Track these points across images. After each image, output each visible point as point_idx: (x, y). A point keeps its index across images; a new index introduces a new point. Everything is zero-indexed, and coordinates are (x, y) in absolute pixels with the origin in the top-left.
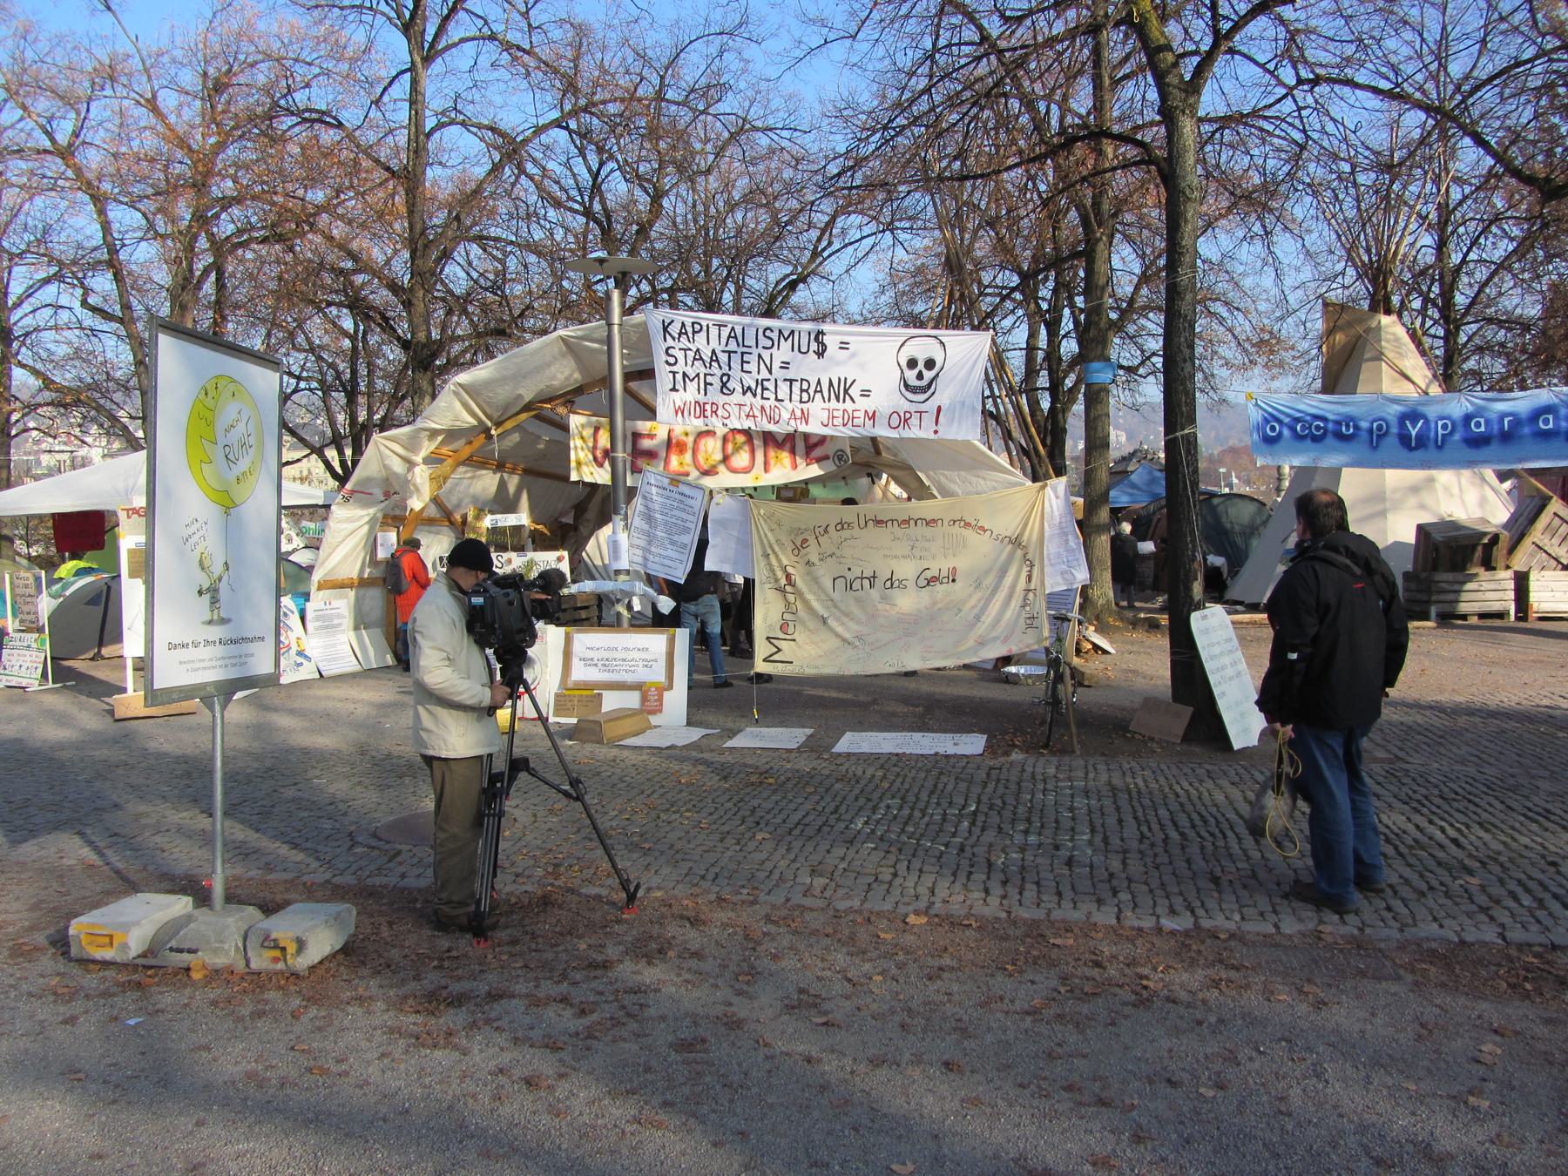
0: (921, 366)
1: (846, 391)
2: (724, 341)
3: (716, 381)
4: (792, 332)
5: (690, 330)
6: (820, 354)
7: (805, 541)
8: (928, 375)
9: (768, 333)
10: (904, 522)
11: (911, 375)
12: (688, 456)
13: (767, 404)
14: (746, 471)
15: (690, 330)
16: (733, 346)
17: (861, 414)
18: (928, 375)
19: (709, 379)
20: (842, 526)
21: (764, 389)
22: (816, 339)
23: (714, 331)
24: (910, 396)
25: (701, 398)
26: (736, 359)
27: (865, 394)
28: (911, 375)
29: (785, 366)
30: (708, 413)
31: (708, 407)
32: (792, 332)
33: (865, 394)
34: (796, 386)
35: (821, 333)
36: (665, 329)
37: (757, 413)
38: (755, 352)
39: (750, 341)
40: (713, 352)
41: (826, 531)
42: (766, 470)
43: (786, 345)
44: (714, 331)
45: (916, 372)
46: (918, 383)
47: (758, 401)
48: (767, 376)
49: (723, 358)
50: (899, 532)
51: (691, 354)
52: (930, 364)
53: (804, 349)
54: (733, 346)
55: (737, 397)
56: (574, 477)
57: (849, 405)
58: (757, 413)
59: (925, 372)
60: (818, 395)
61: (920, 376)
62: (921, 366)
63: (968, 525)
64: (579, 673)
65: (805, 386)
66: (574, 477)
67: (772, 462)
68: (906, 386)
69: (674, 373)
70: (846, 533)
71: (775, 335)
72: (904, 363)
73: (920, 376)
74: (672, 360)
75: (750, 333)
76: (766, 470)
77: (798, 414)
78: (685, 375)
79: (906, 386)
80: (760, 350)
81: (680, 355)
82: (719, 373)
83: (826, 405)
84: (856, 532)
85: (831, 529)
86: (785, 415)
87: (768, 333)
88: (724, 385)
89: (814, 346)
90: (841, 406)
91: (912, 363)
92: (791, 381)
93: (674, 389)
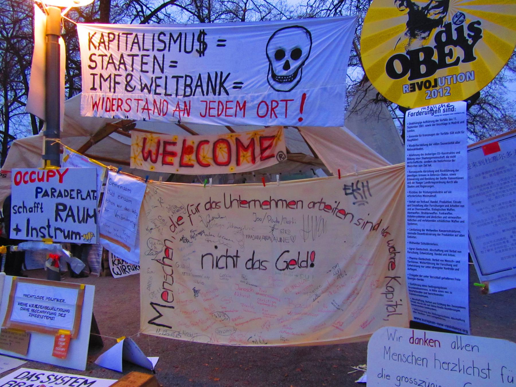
0: (288, 56)
1: (222, 84)
2: (129, 46)
3: (121, 80)
4: (180, 34)
5: (106, 39)
6: (201, 53)
7: (180, 218)
8: (294, 65)
9: (162, 37)
10: (266, 203)
11: (278, 66)
12: (193, 157)
13: (157, 98)
14: (227, 164)
15: (106, 39)
16: (135, 51)
17: (233, 105)
18: (294, 65)
19: (118, 79)
20: (211, 205)
21: (157, 86)
22: (199, 40)
23: (123, 38)
24: (278, 86)
25: (111, 95)
26: (138, 60)
27: (238, 86)
28: (278, 66)
29: (174, 64)
30: (115, 108)
31: (115, 102)
32: (180, 34)
33: (238, 86)
34: (182, 81)
35: (203, 33)
36: (90, 41)
37: (151, 107)
38: (151, 53)
39: (148, 45)
40: (122, 56)
41: (197, 210)
42: (238, 164)
43: (175, 47)
44: (123, 38)
45: (283, 62)
46: (285, 73)
47: (151, 97)
48: (160, 75)
49: (128, 60)
50: (261, 212)
51: (106, 59)
52: (296, 54)
53: (189, 49)
54: (135, 51)
55: (137, 94)
57: (223, 97)
58: (151, 107)
59: (291, 61)
60: (199, 90)
61: (287, 66)
62: (288, 56)
63: (328, 207)
64: (20, 316)
65: (188, 82)
67: (241, 159)
68: (274, 76)
69: (94, 75)
70: (214, 212)
71: (166, 39)
72: (272, 52)
73: (287, 66)
74: (93, 65)
75: (149, 37)
76: (238, 164)
77: (182, 106)
78: (101, 76)
79: (274, 76)
80: (156, 52)
81: (98, 59)
82: (124, 74)
83: (205, 98)
84: (222, 211)
85: (201, 208)
86: (172, 108)
87: (162, 37)
88: (128, 84)
89: (197, 46)
90: (216, 98)
91: (280, 54)
92: (177, 78)
93: (94, 89)
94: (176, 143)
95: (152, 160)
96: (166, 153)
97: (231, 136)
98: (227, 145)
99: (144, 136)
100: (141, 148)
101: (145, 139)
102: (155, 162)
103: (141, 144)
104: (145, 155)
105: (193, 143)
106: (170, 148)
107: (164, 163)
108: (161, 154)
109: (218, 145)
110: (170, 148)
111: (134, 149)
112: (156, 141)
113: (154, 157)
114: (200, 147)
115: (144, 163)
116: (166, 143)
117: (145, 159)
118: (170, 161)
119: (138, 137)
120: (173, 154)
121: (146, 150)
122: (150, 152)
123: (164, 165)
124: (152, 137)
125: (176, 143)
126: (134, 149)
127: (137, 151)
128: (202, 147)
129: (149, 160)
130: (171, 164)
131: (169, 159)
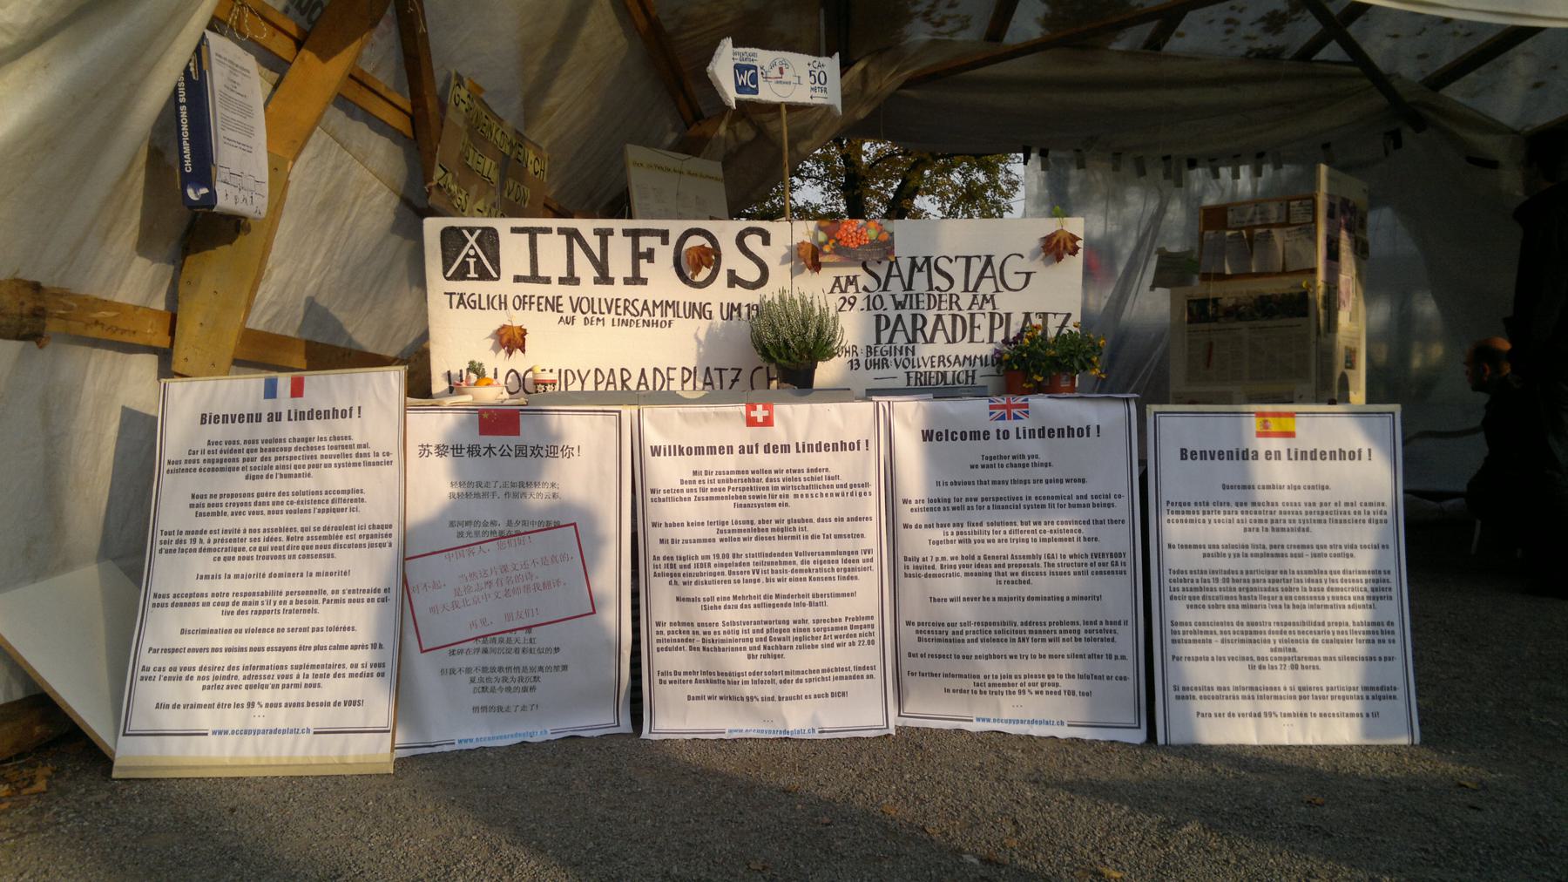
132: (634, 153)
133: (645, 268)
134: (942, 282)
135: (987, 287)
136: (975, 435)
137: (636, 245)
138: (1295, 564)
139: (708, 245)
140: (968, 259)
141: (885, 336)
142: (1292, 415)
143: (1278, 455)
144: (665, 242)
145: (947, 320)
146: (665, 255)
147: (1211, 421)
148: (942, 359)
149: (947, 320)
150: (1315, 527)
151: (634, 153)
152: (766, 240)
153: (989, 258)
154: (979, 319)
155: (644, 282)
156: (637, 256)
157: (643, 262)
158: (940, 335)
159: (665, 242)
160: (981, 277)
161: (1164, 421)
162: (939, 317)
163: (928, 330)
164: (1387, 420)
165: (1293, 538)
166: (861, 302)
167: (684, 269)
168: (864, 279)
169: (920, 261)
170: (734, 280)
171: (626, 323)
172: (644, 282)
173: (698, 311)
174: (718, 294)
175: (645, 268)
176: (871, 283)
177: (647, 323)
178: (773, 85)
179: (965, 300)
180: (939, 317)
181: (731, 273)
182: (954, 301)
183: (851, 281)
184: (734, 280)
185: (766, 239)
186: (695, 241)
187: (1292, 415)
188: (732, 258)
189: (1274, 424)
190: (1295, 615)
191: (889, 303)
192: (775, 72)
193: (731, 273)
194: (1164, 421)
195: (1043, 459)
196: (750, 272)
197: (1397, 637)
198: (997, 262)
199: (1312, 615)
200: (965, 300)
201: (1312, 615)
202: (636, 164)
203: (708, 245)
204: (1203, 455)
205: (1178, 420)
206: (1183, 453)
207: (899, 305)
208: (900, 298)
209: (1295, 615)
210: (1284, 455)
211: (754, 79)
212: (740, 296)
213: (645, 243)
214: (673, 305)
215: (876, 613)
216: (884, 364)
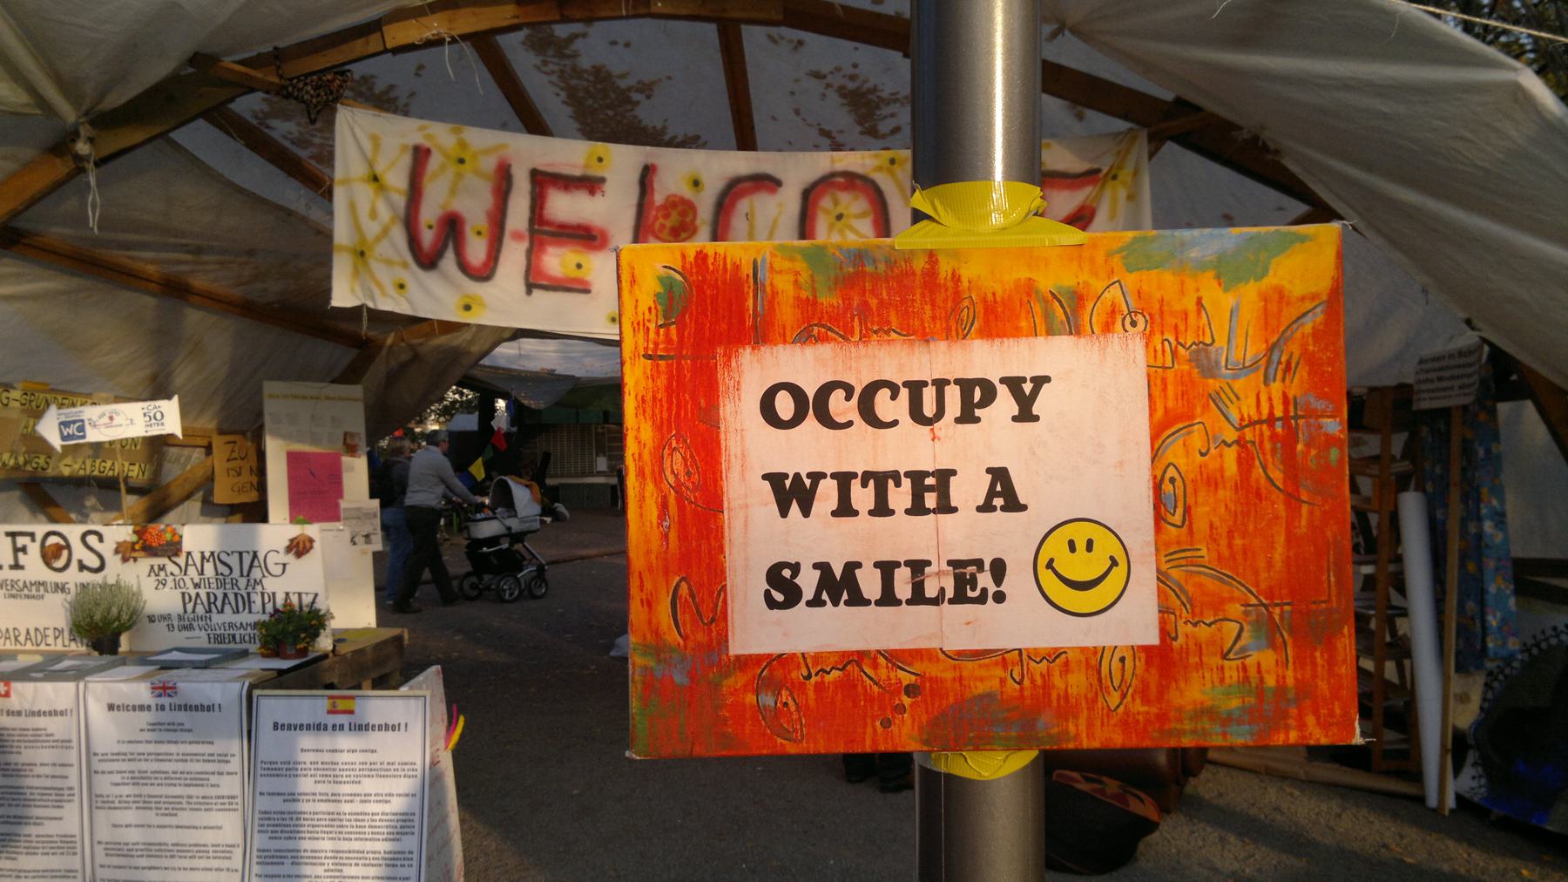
56: (343, 296)
66: (343, 296)
94: (603, 180)
95: (464, 267)
96: (544, 231)
97: (892, 161)
98: (872, 202)
99: (418, 139)
100: (401, 201)
101: (420, 155)
102: (484, 274)
103: (397, 179)
104: (427, 238)
105: (696, 183)
106: (564, 206)
107: (535, 281)
108: (517, 236)
109: (826, 202)
110: (564, 206)
111: (352, 208)
112: (489, 164)
113: (477, 250)
114: (733, 204)
115: (414, 276)
116: (542, 181)
117: (428, 261)
118: (573, 273)
119: (375, 140)
120: (587, 237)
121: (430, 213)
122: (452, 226)
123: (537, 293)
124: (463, 145)
125: (603, 180)
126: (352, 208)
127: (374, 215)
128: (743, 205)
129: (449, 261)
130: (578, 287)
131: (558, 260)
132: (270, 387)
133: (22, 558)
134: (221, 568)
135: (256, 574)
136: (142, 708)
137: (14, 543)
138: (347, 808)
139: (62, 543)
140: (241, 554)
141: (190, 607)
142: (352, 698)
143: (342, 727)
144: (33, 540)
145: (232, 597)
146: (34, 549)
147: (296, 701)
148: (231, 625)
149: (232, 597)
150: (365, 781)
151: (270, 387)
152: (101, 539)
153: (255, 553)
154: (253, 597)
155: (22, 568)
156: (16, 550)
157: (20, 555)
158: (227, 607)
159: (33, 540)
160: (251, 566)
161: (263, 701)
162: (225, 595)
163: (219, 603)
164: (420, 702)
165: (347, 789)
166: (170, 583)
167: (49, 556)
168: (171, 567)
169: (207, 555)
170: (82, 567)
171: (13, 596)
172: (22, 568)
173: (60, 588)
174: (73, 577)
175: (22, 558)
176: (176, 570)
177: (27, 597)
178: (103, 429)
179: (242, 582)
180: (225, 595)
181: (80, 562)
182: (234, 584)
183: (162, 568)
184: (82, 567)
185: (101, 539)
186: (53, 540)
187: (352, 698)
188: (79, 552)
189: (341, 705)
190: (345, 845)
191: (189, 584)
192: (106, 420)
193: (80, 562)
194: (263, 701)
195: (187, 726)
196: (93, 562)
197: (415, 863)
198: (261, 556)
199: (357, 845)
200: (242, 582)
201: (357, 845)
202: (271, 396)
203: (62, 543)
204: (289, 726)
205: (272, 701)
206: (276, 726)
207: (197, 586)
208: (197, 580)
209: (345, 845)
210: (346, 727)
211: (81, 429)
212: (86, 577)
213: (21, 541)
214: (43, 584)
215: (76, 831)
216: (190, 628)
